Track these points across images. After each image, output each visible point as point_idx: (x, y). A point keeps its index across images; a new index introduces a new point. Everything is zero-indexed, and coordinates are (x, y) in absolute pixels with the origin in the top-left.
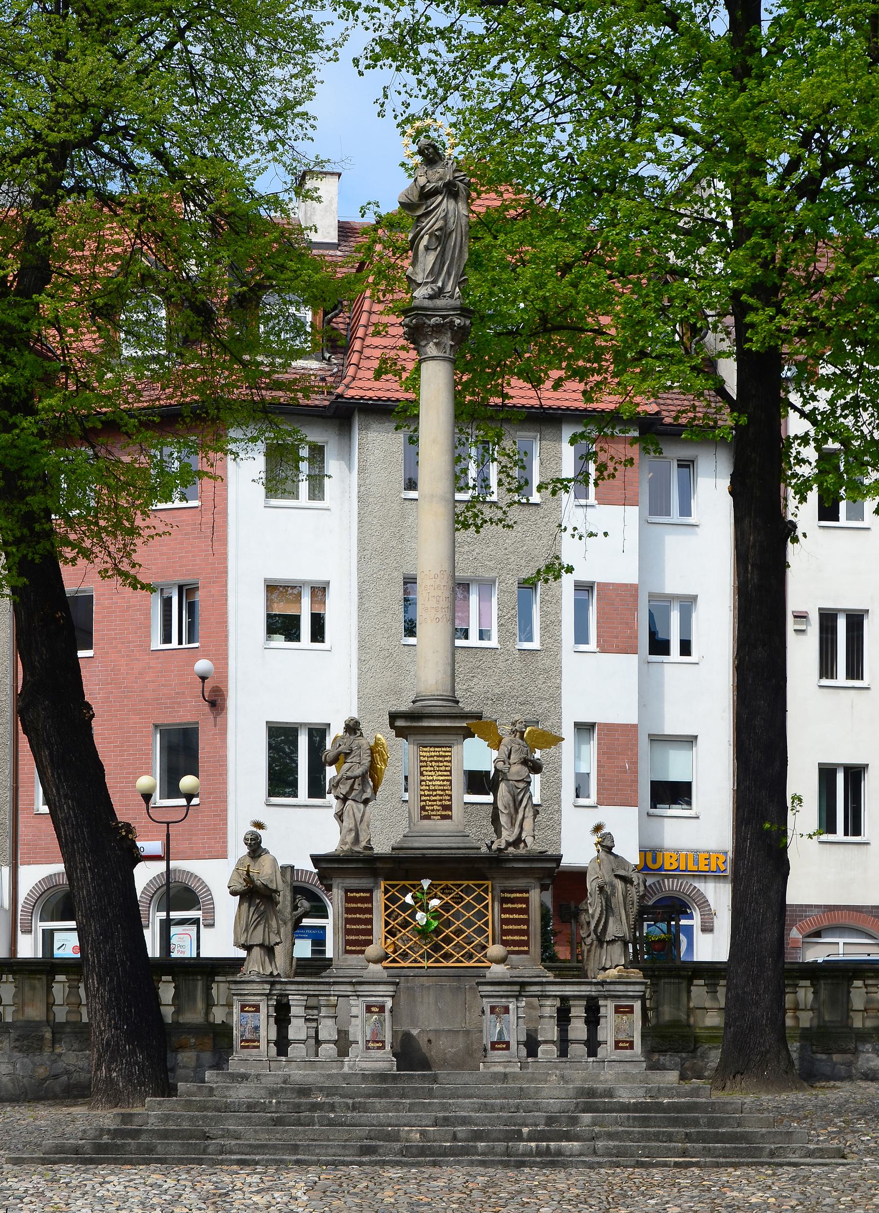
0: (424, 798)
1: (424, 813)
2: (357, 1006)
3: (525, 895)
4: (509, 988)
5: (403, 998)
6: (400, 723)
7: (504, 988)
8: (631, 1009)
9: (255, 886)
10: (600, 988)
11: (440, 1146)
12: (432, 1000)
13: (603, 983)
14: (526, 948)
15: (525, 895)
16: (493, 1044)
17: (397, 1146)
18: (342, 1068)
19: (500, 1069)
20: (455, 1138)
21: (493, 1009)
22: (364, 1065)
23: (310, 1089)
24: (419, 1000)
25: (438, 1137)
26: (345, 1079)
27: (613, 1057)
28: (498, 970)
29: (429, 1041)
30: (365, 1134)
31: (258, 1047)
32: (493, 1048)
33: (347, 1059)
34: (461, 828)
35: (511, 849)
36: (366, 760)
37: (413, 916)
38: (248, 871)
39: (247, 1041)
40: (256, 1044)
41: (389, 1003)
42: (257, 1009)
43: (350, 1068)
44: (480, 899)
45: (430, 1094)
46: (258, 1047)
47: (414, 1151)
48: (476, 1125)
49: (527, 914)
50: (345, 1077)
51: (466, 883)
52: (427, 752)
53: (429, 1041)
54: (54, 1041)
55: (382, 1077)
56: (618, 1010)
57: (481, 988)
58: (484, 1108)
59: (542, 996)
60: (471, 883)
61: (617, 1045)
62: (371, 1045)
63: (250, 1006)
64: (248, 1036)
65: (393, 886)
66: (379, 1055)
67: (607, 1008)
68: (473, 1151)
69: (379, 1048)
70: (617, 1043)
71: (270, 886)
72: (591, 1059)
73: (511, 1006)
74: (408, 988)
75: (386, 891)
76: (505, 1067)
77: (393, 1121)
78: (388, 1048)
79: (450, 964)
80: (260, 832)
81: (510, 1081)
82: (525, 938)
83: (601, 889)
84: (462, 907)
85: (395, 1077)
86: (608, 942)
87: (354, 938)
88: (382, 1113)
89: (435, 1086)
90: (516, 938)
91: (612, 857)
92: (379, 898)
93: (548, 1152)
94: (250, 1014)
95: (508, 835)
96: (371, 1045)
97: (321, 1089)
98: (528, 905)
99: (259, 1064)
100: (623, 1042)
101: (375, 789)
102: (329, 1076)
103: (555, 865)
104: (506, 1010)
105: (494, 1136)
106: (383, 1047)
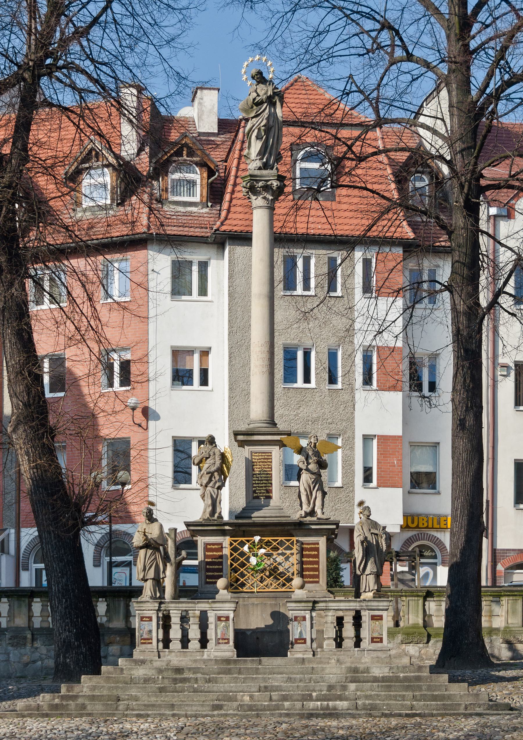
3: (316, 546)
5: (241, 611)
7: (303, 604)
10: (362, 604)
11: (261, 705)
12: (259, 613)
13: (364, 600)
14: (317, 580)
15: (316, 546)
16: (296, 640)
17: (235, 704)
18: (203, 656)
19: (300, 656)
20: (271, 700)
22: (217, 654)
23: (183, 669)
24: (252, 613)
25: (260, 699)
26: (204, 663)
27: (370, 648)
29: (258, 638)
30: (215, 697)
31: (151, 643)
32: (296, 643)
33: (206, 650)
39: (145, 639)
40: (150, 641)
42: (150, 619)
43: (208, 656)
46: (151, 643)
47: (246, 707)
48: (284, 691)
49: (318, 557)
50: (205, 661)
51: (280, 539)
53: (258, 638)
55: (227, 661)
58: (290, 680)
59: (326, 610)
60: (283, 538)
61: (373, 640)
62: (221, 641)
63: (146, 617)
64: (145, 636)
65: (235, 541)
66: (226, 648)
67: (366, 616)
69: (226, 643)
70: (372, 639)
72: (356, 649)
74: (244, 605)
75: (231, 544)
76: (304, 654)
77: (233, 689)
78: (232, 643)
79: (270, 590)
81: (306, 663)
82: (317, 573)
85: (235, 661)
88: (226, 684)
89: (260, 667)
94: (146, 623)
96: (221, 641)
97: (190, 669)
98: (318, 552)
99: (152, 654)
100: (376, 638)
102: (195, 661)
104: (304, 618)
105: (295, 698)
106: (228, 643)
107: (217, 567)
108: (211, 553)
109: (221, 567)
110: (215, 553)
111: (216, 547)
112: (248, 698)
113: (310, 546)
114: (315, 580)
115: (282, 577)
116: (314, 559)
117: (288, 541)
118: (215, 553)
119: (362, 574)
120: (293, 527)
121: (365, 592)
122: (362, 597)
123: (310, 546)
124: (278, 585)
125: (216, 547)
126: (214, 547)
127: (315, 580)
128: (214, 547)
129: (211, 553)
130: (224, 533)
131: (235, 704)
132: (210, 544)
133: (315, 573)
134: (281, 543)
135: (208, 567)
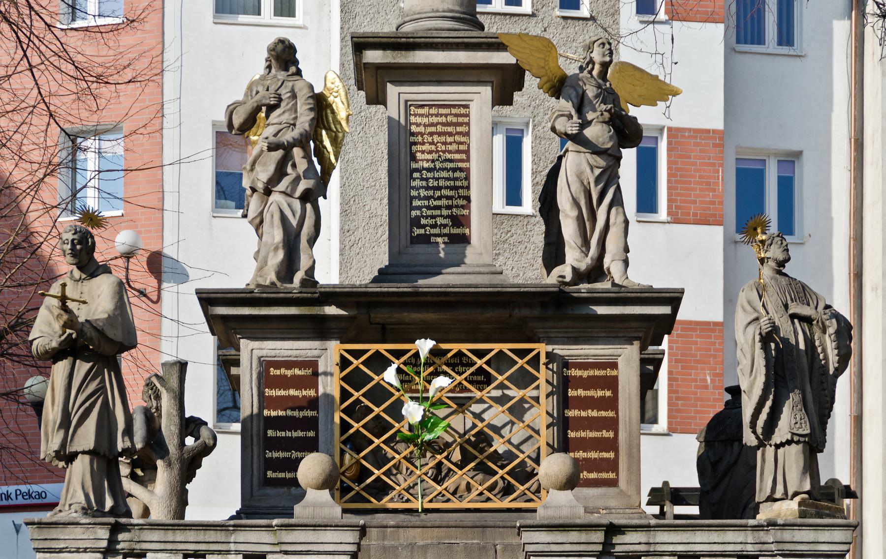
0: (416, 203)
1: (418, 231)
3: (610, 372)
4: (583, 537)
6: (373, 56)
7: (574, 536)
9: (81, 333)
10: (762, 536)
13: (772, 524)
14: (612, 475)
15: (610, 372)
28: (558, 503)
34: (487, 259)
35: (584, 287)
36: (305, 119)
37: (396, 411)
38: (63, 299)
49: (615, 408)
51: (496, 347)
57: (527, 536)
60: (505, 347)
65: (357, 354)
71: (110, 333)
74: (385, 549)
75: (344, 363)
79: (465, 505)
80: (94, 232)
82: (611, 455)
83: (766, 339)
84: (488, 363)
86: (777, 447)
87: (281, 455)
90: (593, 455)
91: (783, 280)
95: (575, 258)
103: (666, 310)
107: (300, 434)
108: (282, 393)
109: (311, 434)
110: (292, 392)
111: (297, 372)
113: (591, 373)
114: (604, 475)
115: (502, 467)
116: (603, 414)
117: (521, 353)
118: (292, 392)
119: (761, 444)
120: (537, 312)
121: (771, 499)
122: (762, 517)
123: (591, 373)
124: (491, 489)
125: (297, 372)
126: (289, 373)
127: (604, 475)
128: (289, 373)
129: (282, 393)
130: (320, 329)
132: (278, 365)
133: (605, 455)
135: (270, 433)
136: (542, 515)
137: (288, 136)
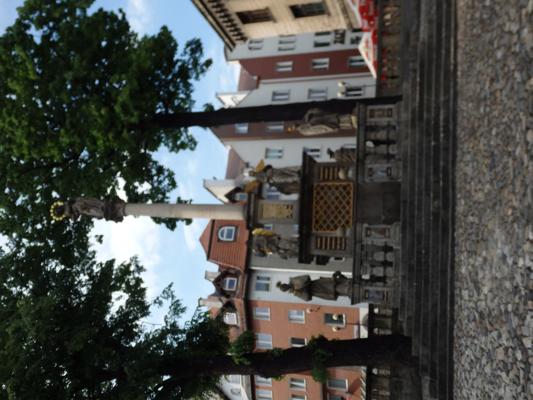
2: (367, 241)
8: (372, 111)
17: (442, 212)
18: (399, 250)
21: (370, 175)
22: (397, 238)
28: (351, 174)
40: (385, 293)
41: (366, 225)
42: (367, 291)
44: (322, 188)
45: (412, 203)
52: (265, 215)
54: (397, 376)
56: (372, 116)
65: (315, 227)
68: (445, 169)
73: (369, 166)
75: (317, 230)
78: (389, 226)
92: (321, 232)
93: (446, 127)
101: (275, 235)
104: (371, 169)
112: (436, 202)
117: (316, 189)
121: (352, 123)
131: (442, 212)
134: (318, 193)
136: (354, 178)
137: (265, 242)
